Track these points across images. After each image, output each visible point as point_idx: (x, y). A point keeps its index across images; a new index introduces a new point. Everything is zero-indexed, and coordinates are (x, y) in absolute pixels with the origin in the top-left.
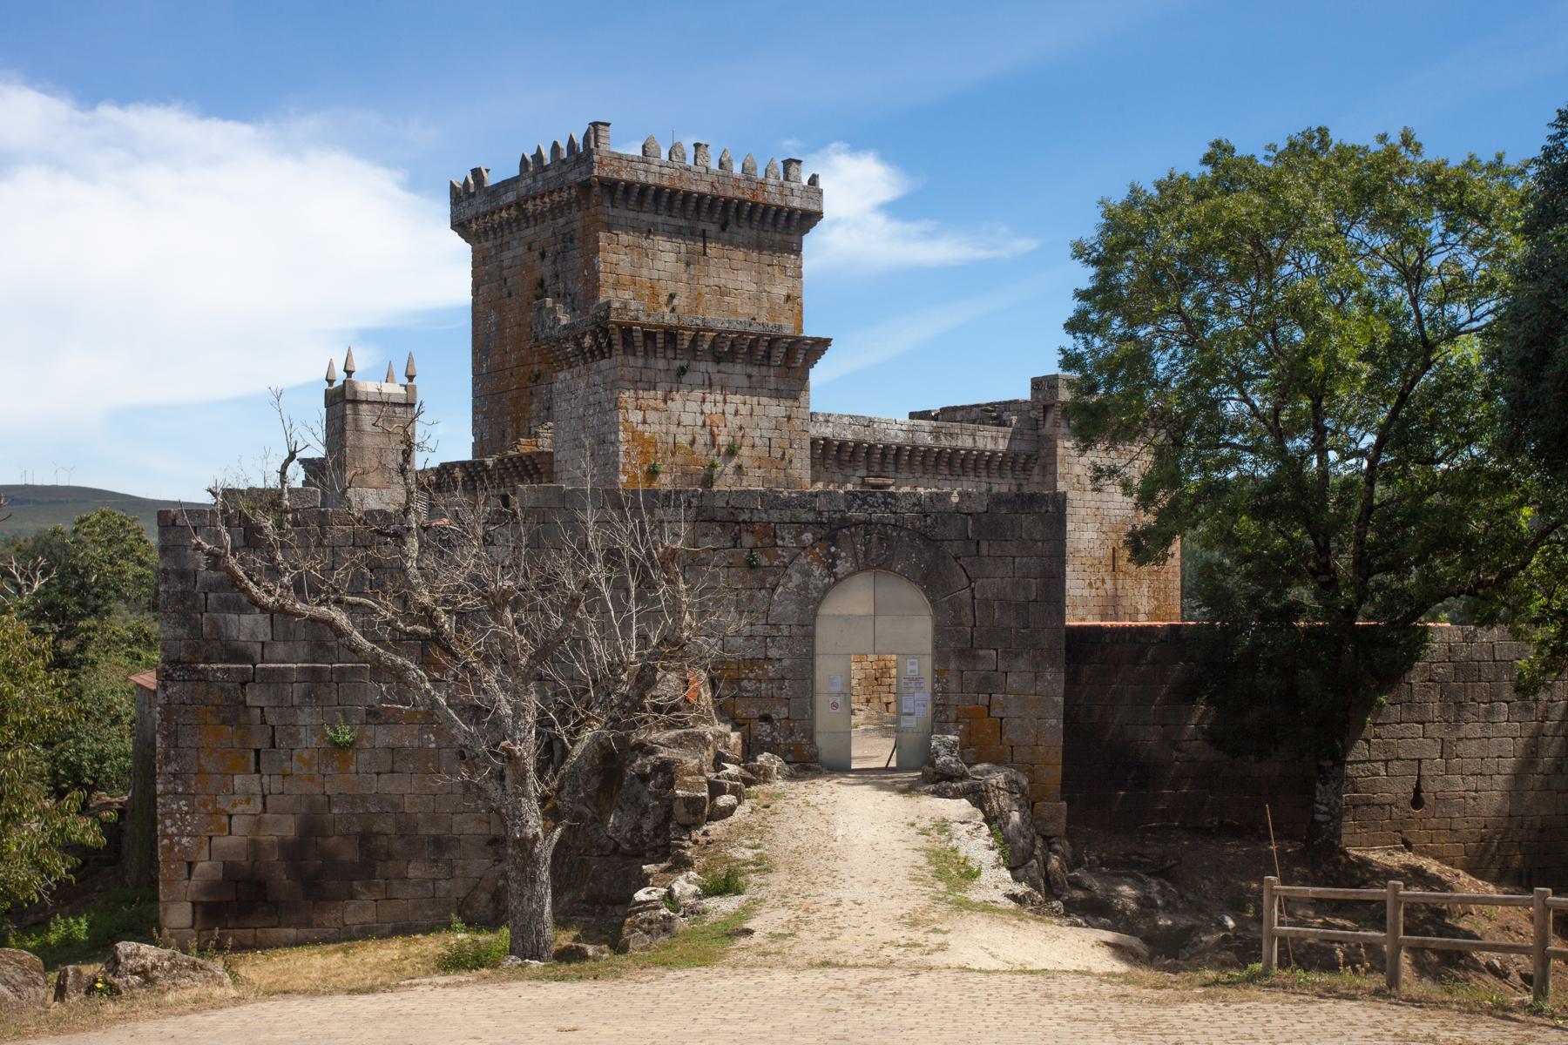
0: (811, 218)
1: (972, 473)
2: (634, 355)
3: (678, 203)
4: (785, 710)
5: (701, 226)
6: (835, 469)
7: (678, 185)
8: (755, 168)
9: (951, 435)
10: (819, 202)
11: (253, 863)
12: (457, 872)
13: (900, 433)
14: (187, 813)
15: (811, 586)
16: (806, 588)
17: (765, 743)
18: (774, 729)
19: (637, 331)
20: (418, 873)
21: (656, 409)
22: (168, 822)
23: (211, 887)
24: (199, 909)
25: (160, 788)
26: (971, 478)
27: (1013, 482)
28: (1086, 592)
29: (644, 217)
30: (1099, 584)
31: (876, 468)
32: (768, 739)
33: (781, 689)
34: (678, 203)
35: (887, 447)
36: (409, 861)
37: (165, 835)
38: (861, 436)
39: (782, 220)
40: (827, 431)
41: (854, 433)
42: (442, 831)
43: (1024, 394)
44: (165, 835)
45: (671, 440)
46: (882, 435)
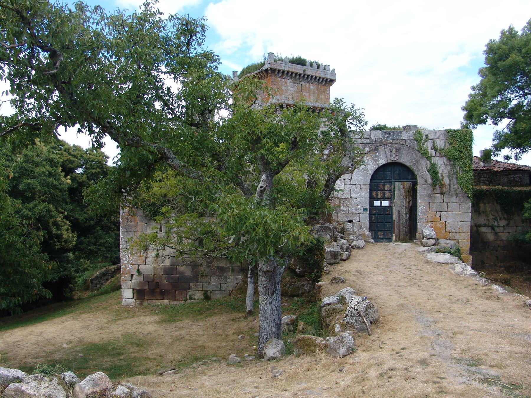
0: (332, 81)
3: (293, 76)
4: (358, 218)
5: (301, 83)
7: (294, 71)
10: (335, 78)
11: (154, 275)
12: (229, 281)
14: (131, 256)
15: (368, 169)
16: (367, 170)
17: (351, 232)
18: (354, 226)
20: (214, 281)
22: (124, 259)
23: (140, 284)
24: (135, 291)
25: (121, 246)
29: (283, 80)
32: (352, 230)
33: (357, 210)
34: (293, 76)
36: (211, 276)
37: (123, 264)
39: (324, 81)
42: (223, 265)
44: (123, 264)
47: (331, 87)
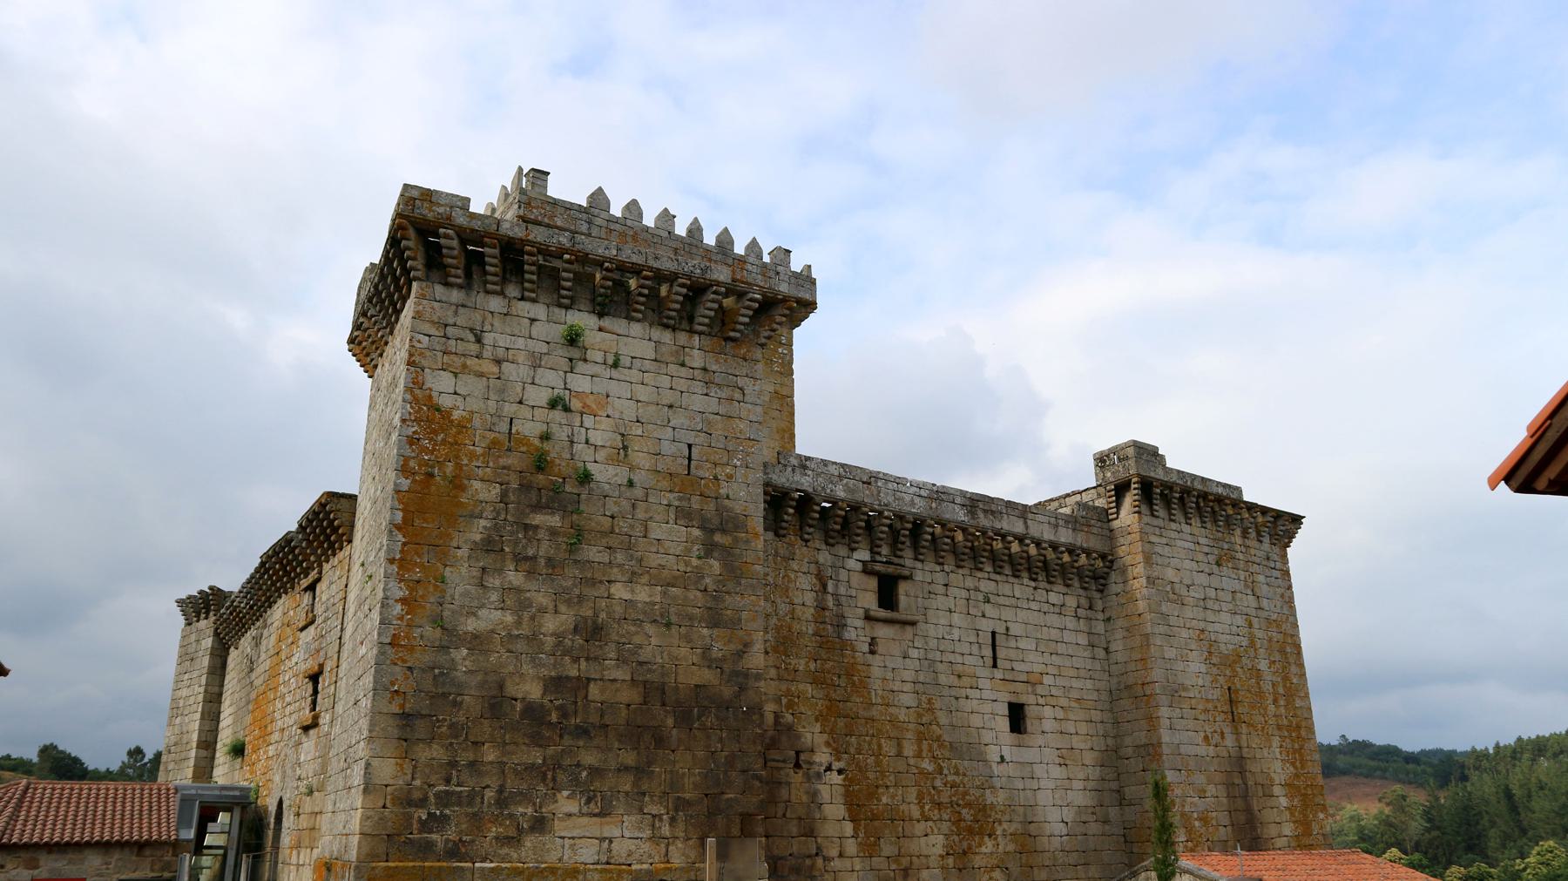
1: (1025, 574)
2: (447, 284)
6: (818, 544)
8: (732, 243)
9: (993, 512)
13: (917, 500)
19: (447, 236)
21: (481, 375)
26: (1026, 581)
27: (1081, 592)
28: (1202, 750)
30: (1217, 737)
31: (885, 550)
35: (900, 517)
38: (859, 497)
40: (805, 482)
41: (847, 489)
43: (1087, 477)
45: (504, 427)
46: (891, 499)
47: (796, 331)
